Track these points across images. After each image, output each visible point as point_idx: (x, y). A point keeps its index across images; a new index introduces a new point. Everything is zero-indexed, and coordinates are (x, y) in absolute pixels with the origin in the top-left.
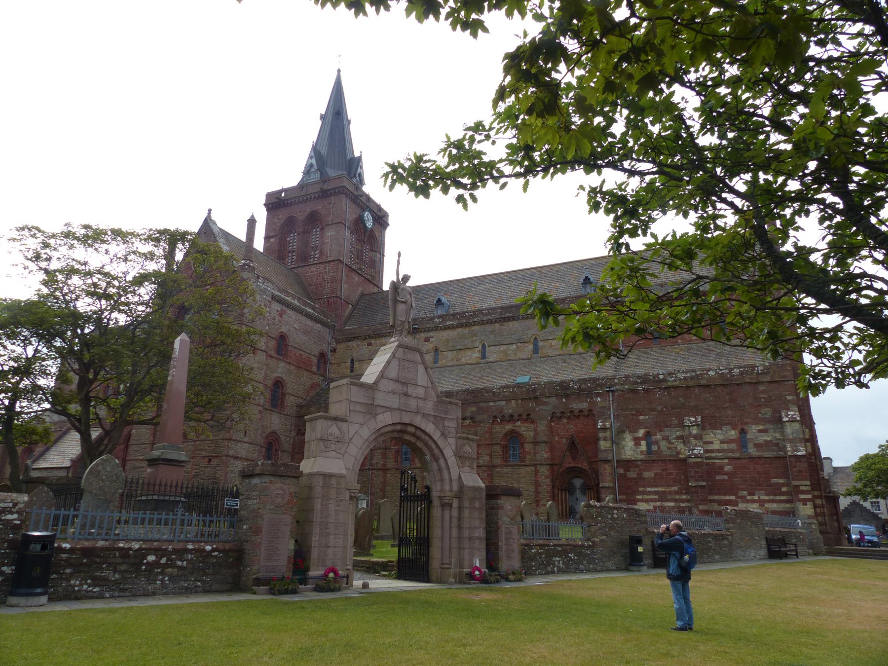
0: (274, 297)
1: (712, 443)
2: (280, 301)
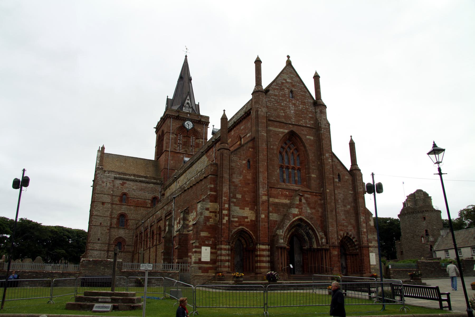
0: (115, 178)
1: (190, 222)
2: (121, 179)
